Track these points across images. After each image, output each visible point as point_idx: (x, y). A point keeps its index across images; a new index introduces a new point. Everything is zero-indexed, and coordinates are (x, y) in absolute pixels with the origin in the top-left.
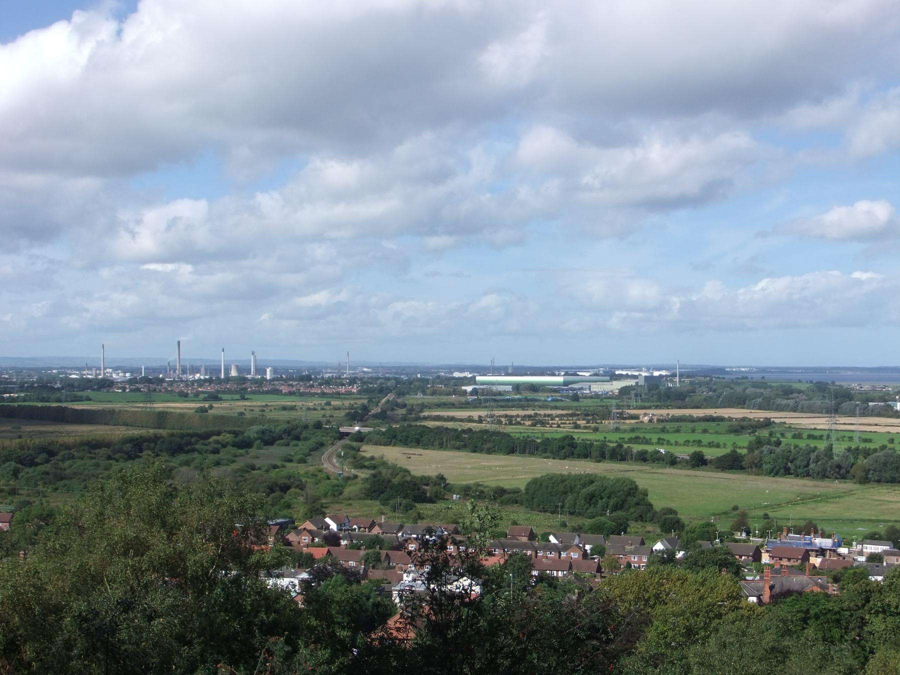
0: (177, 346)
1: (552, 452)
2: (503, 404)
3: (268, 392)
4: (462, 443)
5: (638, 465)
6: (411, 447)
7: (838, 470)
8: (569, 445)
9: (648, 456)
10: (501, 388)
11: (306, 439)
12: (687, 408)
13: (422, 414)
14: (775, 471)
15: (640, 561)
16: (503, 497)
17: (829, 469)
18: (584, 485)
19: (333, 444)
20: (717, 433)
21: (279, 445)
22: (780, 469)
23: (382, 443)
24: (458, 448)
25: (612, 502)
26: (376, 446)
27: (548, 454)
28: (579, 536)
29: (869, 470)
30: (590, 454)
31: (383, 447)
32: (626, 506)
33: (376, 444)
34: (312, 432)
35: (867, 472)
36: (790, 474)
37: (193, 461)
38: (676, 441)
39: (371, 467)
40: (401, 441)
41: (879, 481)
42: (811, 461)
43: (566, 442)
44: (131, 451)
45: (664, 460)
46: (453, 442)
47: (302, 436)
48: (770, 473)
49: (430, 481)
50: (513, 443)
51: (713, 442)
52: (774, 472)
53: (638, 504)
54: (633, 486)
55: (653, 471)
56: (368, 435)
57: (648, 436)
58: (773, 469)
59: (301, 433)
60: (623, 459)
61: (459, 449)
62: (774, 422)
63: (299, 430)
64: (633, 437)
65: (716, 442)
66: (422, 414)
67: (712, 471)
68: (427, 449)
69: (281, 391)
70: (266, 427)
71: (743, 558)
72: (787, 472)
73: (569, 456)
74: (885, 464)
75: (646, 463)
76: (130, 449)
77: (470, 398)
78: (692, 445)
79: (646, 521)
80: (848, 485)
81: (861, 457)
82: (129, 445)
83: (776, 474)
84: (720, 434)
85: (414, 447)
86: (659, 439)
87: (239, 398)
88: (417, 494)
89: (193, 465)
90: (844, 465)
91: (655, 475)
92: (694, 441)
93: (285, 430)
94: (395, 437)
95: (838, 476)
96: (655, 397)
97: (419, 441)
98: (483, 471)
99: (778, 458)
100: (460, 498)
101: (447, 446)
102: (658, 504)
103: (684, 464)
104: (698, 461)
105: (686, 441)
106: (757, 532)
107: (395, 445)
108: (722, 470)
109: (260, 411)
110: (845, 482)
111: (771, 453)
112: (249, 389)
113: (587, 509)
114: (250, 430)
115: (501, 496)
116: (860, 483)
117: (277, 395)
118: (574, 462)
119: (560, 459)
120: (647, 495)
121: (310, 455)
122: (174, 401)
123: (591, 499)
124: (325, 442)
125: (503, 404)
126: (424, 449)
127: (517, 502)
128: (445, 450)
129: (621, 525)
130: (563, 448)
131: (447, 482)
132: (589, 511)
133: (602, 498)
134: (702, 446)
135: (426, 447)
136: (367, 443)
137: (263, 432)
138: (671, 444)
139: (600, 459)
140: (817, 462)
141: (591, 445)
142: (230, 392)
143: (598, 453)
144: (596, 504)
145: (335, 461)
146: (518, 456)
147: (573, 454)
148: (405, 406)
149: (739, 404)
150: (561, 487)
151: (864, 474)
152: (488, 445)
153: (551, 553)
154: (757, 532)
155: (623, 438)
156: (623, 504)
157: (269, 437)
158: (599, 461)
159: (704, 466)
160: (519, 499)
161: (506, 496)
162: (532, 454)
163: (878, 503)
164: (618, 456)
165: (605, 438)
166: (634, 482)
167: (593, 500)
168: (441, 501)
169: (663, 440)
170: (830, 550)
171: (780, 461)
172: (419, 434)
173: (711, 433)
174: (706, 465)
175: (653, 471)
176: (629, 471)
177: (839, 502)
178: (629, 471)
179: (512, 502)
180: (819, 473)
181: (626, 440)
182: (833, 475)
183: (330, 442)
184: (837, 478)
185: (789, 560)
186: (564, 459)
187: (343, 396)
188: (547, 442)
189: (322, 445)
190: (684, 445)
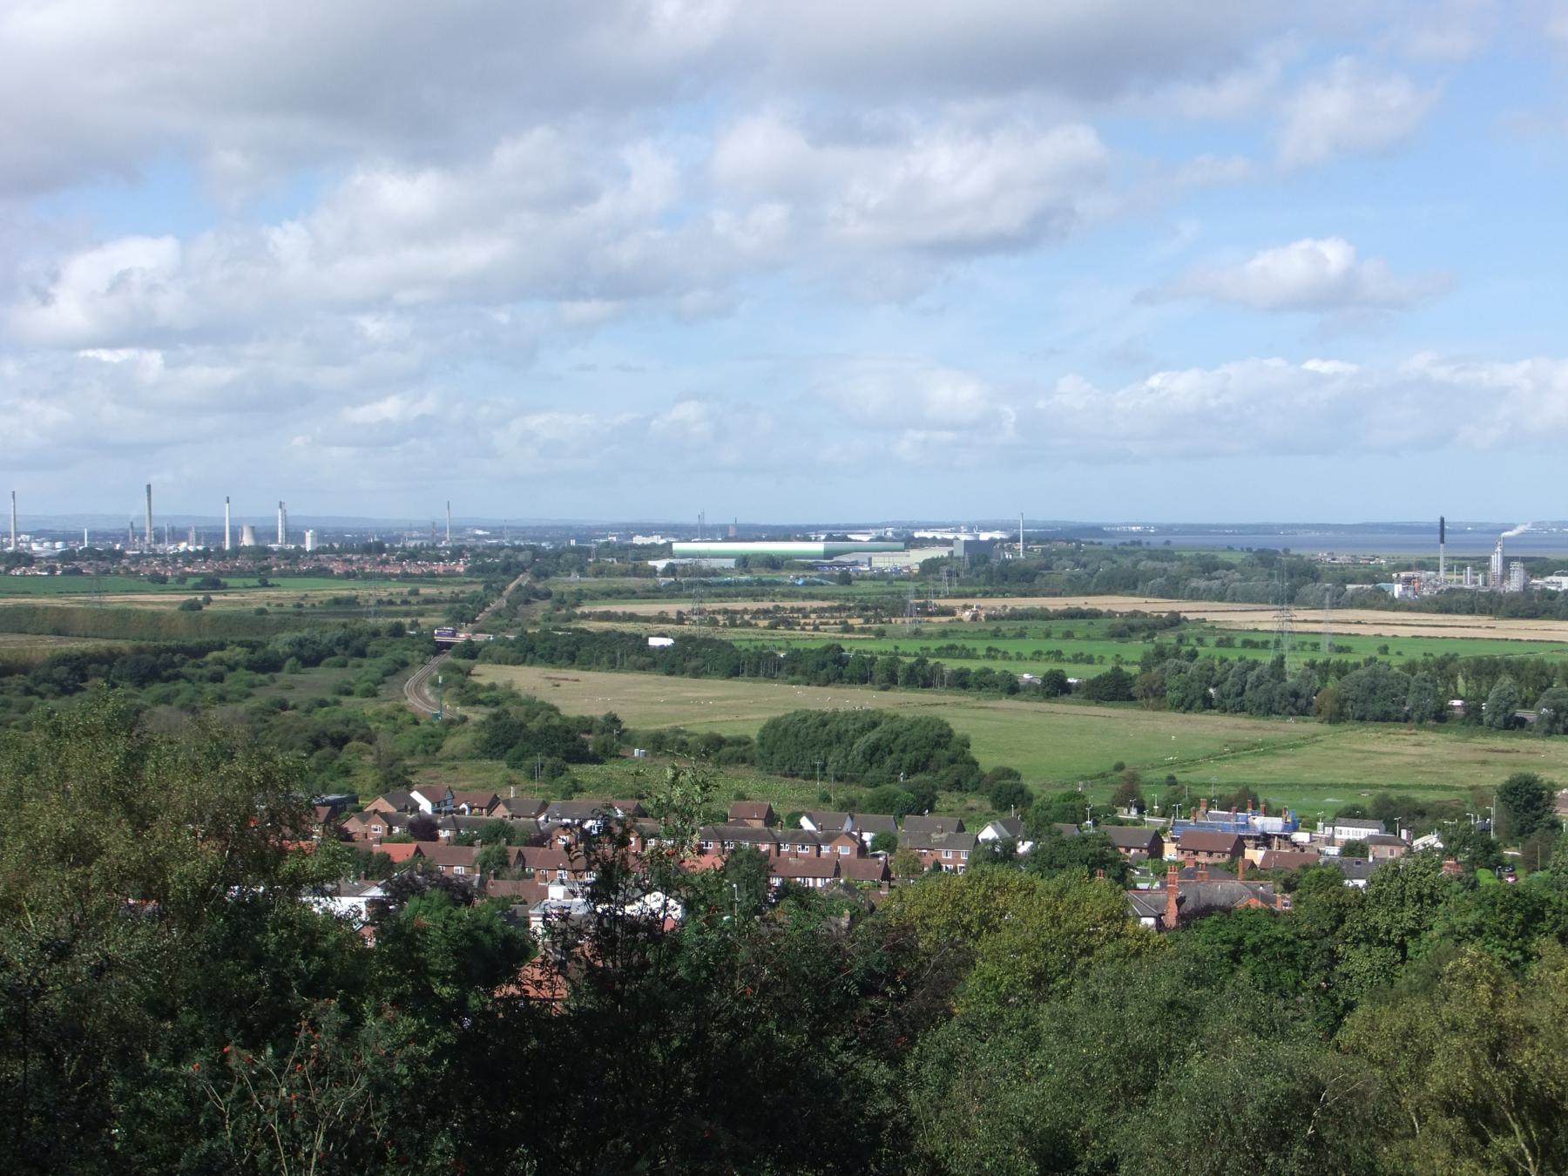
0: (146, 494)
1: (804, 673)
2: (719, 590)
3: (307, 574)
4: (649, 660)
5: (953, 694)
6: (560, 667)
7: (1293, 700)
8: (835, 661)
9: (971, 679)
10: (716, 563)
11: (376, 655)
12: (1036, 596)
13: (578, 611)
14: (1186, 703)
15: (957, 858)
16: (720, 752)
17: (1277, 698)
18: (862, 731)
19: (423, 663)
20: (1088, 638)
21: (327, 665)
22: (1195, 699)
23: (510, 661)
24: (642, 669)
25: (908, 758)
26: (499, 666)
27: (797, 677)
28: (852, 818)
29: (1346, 700)
30: (871, 676)
31: (512, 667)
32: (933, 765)
33: (500, 661)
34: (387, 642)
35: (1342, 702)
36: (1212, 708)
37: (177, 695)
38: (1018, 653)
39: (490, 701)
40: (542, 656)
41: (1362, 719)
42: (1247, 687)
43: (830, 655)
44: (66, 679)
45: (997, 685)
46: (633, 658)
47: (369, 649)
48: (1178, 707)
49: (594, 725)
50: (738, 658)
51: (1082, 654)
52: (1185, 705)
53: (952, 761)
54: (945, 732)
56: (484, 646)
57: (969, 644)
58: (1183, 700)
59: (366, 644)
60: (927, 684)
61: (644, 669)
62: (1185, 619)
63: (364, 639)
64: (945, 646)
65: (1086, 653)
66: (578, 611)
67: (1080, 704)
68: (589, 670)
69: (332, 572)
70: (305, 633)
71: (1133, 851)
72: (1208, 704)
73: (834, 681)
74: (1373, 691)
75: (962, 691)
76: (65, 676)
77: (663, 581)
78: (1047, 660)
79: (967, 791)
80: (1310, 726)
81: (1332, 677)
82: (63, 668)
83: (1189, 708)
84: (1094, 639)
85: (565, 667)
86: (990, 649)
87: (259, 584)
88: (571, 747)
89: (178, 701)
90: (1304, 691)
91: (982, 712)
92: (1049, 653)
93: (339, 639)
94: (532, 649)
95: (1294, 711)
96: (982, 578)
97: (575, 657)
98: (686, 707)
99: (1193, 681)
100: (646, 754)
101: (622, 664)
102: (988, 762)
103: (1032, 692)
104: (1056, 687)
105: (1035, 653)
106: (1156, 807)
107: (532, 664)
108: (1097, 702)
109: (294, 606)
110: (1306, 722)
111: (1180, 672)
112: (275, 569)
113: (865, 771)
114: (277, 640)
115: (717, 751)
116: (1331, 722)
117: (325, 577)
118: (842, 690)
119: (819, 685)
120: (968, 746)
121: (384, 682)
122: (141, 592)
123: (874, 754)
124: (410, 660)
125: (719, 590)
126: (583, 670)
127: (744, 760)
128: (619, 671)
129: (924, 797)
130: (824, 666)
131: (623, 727)
132: (869, 774)
133: (891, 752)
134: (1064, 660)
135: (586, 667)
136: (484, 661)
137: (301, 644)
138: (1010, 659)
139: (888, 684)
140: (1257, 687)
141: (873, 660)
142: (241, 573)
143: (884, 675)
144: (881, 762)
145: (427, 692)
146: (747, 681)
147: (840, 676)
148: (548, 595)
149: (1127, 587)
150: (823, 734)
151: (1337, 706)
152: (693, 663)
153: (803, 848)
154: (1156, 807)
155: (928, 649)
156: (928, 760)
157: (310, 652)
158: (885, 689)
159: (1066, 695)
160: (748, 754)
161: (726, 750)
162: (771, 677)
163: (1360, 755)
164: (920, 679)
165: (896, 648)
166: (947, 725)
167: (878, 755)
168: (613, 759)
169: (996, 650)
170: (1279, 836)
171: (1196, 685)
172: (574, 643)
173: (1079, 639)
174: (1070, 693)
176: (937, 704)
177: (1293, 755)
178: (937, 704)
179: (737, 761)
180: (1260, 705)
181: (933, 651)
182: (1284, 708)
183: (419, 660)
184: (1291, 714)
185: (1210, 853)
186: (824, 686)
187: (441, 580)
188: (796, 657)
189: (404, 664)
190: (1032, 659)
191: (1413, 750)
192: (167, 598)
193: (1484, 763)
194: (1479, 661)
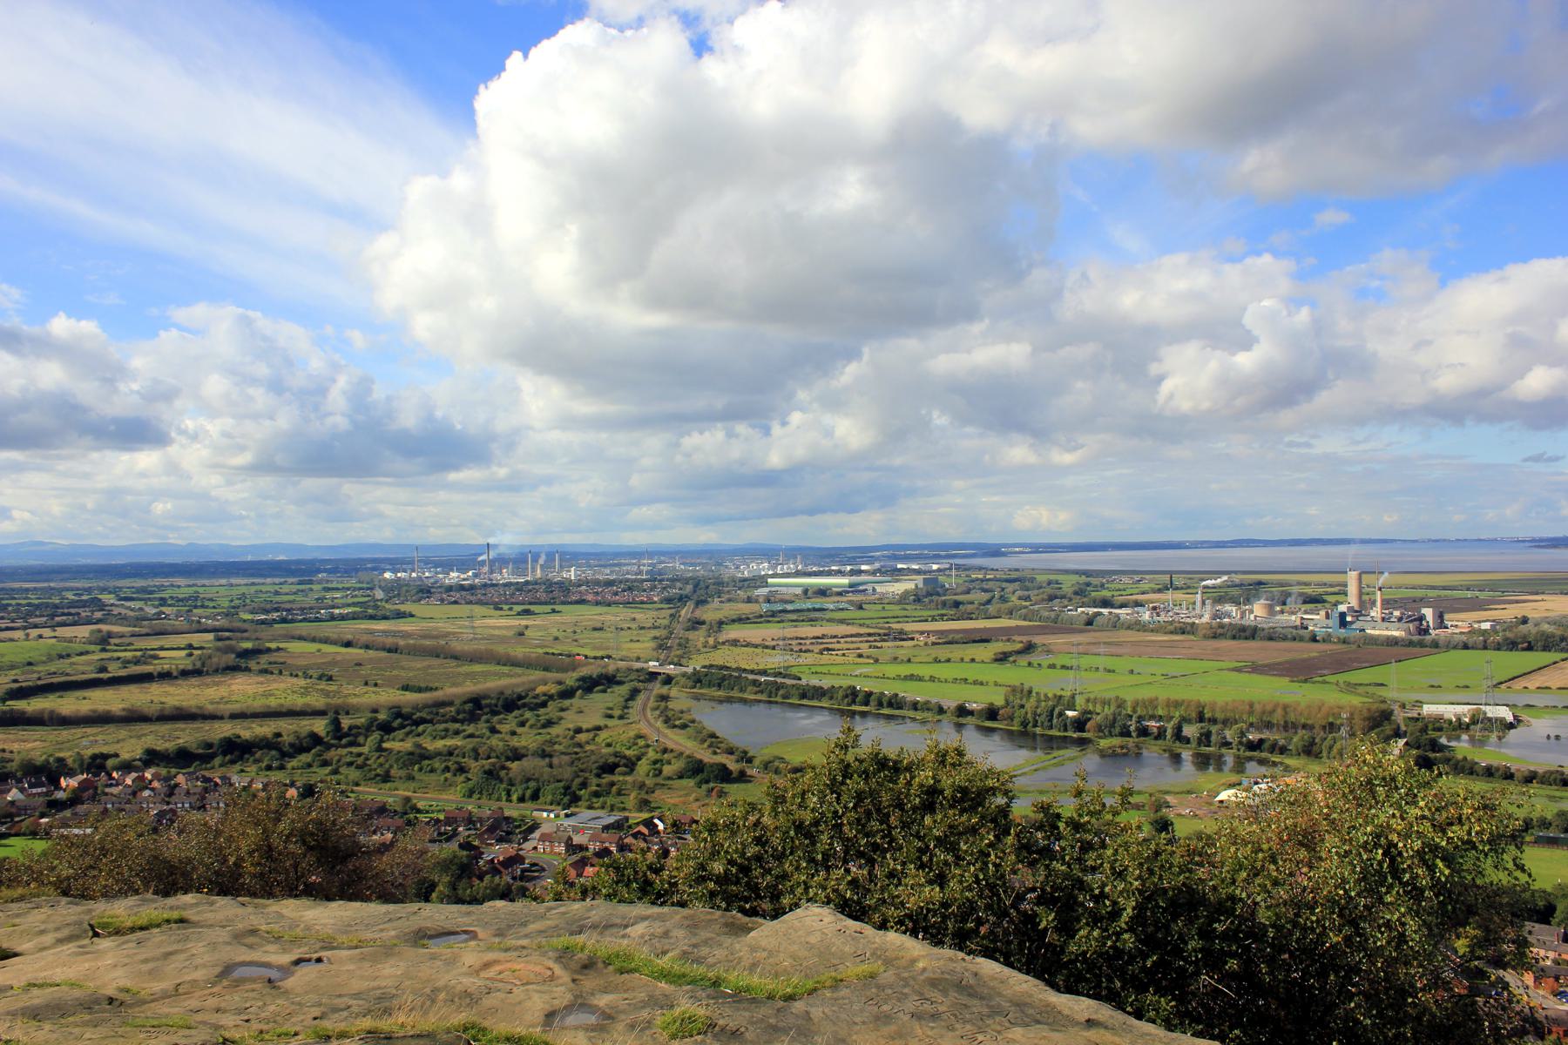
2: (794, 617)
9: (919, 706)
10: (791, 590)
13: (722, 637)
20: (983, 662)
21: (597, 692)
43: (849, 692)
46: (750, 688)
66: (722, 637)
77: (765, 607)
89: (528, 724)
96: (933, 607)
125: (794, 617)
148: (703, 623)
192: (503, 622)
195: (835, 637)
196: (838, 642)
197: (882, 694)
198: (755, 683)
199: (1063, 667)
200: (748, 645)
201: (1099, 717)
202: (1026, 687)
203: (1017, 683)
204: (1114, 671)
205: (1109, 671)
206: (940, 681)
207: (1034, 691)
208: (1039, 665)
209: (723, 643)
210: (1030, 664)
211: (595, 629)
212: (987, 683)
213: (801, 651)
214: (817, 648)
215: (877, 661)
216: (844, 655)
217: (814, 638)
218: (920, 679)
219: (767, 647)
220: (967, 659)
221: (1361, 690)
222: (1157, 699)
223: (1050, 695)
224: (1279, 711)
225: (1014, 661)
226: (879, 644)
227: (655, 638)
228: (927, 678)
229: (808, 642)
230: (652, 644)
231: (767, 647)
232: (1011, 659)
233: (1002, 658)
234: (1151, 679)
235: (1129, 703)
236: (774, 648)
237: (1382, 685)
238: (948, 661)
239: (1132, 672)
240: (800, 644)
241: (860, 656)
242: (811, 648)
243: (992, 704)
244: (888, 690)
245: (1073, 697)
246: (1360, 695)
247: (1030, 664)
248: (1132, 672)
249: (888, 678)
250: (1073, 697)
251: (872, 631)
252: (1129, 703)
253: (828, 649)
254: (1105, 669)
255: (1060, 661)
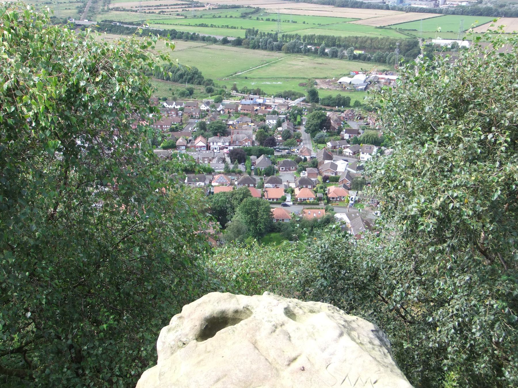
9: (205, 39)
53: (198, 77)
55: (208, 47)
66: (111, 6)
81: (288, 38)
102: (206, 77)
104: (225, 42)
116: (286, 53)
123: (181, 76)
141: (183, 33)
158: (186, 41)
163: (289, 66)
171: (256, 43)
175: (208, 47)
191: (301, 63)
193: (315, 68)
194: (320, 36)
195: (166, 5)
196: (168, 8)
197: (188, 33)
198: (127, 28)
199: (273, 20)
200: (124, 10)
201: (287, 44)
202: (256, 29)
203: (251, 28)
204: (296, 22)
205: (294, 22)
206: (215, 26)
207: (259, 32)
208: (262, 19)
209: (112, 9)
210: (258, 19)
211: (47, 3)
212: (238, 27)
213: (150, 13)
214: (157, 11)
215: (186, 17)
216: (170, 14)
217: (156, 6)
218: (206, 26)
219: (134, 11)
220: (228, 16)
221: (406, 32)
222: (315, 35)
223: (266, 34)
224: (369, 41)
225: (251, 17)
226: (187, 9)
227: (78, 7)
228: (210, 25)
229: (153, 8)
230: (76, 11)
231: (134, 11)
232: (250, 16)
233: (244, 16)
234: (314, 26)
235: (302, 37)
236: (136, 11)
237: (416, 30)
238: (220, 17)
239: (304, 23)
240: (149, 9)
241: (178, 15)
242: (154, 11)
243: (239, 38)
244: (191, 30)
245: (277, 34)
246: (405, 34)
247: (258, 19)
248: (304, 23)
249: (191, 26)
250: (277, 34)
251: (184, 3)
252: (302, 37)
253: (163, 12)
254: (292, 21)
255: (271, 18)
